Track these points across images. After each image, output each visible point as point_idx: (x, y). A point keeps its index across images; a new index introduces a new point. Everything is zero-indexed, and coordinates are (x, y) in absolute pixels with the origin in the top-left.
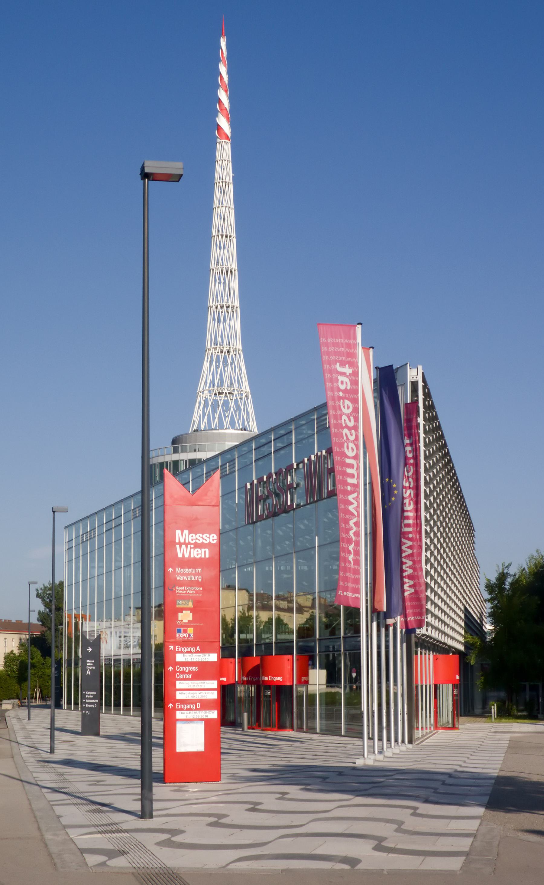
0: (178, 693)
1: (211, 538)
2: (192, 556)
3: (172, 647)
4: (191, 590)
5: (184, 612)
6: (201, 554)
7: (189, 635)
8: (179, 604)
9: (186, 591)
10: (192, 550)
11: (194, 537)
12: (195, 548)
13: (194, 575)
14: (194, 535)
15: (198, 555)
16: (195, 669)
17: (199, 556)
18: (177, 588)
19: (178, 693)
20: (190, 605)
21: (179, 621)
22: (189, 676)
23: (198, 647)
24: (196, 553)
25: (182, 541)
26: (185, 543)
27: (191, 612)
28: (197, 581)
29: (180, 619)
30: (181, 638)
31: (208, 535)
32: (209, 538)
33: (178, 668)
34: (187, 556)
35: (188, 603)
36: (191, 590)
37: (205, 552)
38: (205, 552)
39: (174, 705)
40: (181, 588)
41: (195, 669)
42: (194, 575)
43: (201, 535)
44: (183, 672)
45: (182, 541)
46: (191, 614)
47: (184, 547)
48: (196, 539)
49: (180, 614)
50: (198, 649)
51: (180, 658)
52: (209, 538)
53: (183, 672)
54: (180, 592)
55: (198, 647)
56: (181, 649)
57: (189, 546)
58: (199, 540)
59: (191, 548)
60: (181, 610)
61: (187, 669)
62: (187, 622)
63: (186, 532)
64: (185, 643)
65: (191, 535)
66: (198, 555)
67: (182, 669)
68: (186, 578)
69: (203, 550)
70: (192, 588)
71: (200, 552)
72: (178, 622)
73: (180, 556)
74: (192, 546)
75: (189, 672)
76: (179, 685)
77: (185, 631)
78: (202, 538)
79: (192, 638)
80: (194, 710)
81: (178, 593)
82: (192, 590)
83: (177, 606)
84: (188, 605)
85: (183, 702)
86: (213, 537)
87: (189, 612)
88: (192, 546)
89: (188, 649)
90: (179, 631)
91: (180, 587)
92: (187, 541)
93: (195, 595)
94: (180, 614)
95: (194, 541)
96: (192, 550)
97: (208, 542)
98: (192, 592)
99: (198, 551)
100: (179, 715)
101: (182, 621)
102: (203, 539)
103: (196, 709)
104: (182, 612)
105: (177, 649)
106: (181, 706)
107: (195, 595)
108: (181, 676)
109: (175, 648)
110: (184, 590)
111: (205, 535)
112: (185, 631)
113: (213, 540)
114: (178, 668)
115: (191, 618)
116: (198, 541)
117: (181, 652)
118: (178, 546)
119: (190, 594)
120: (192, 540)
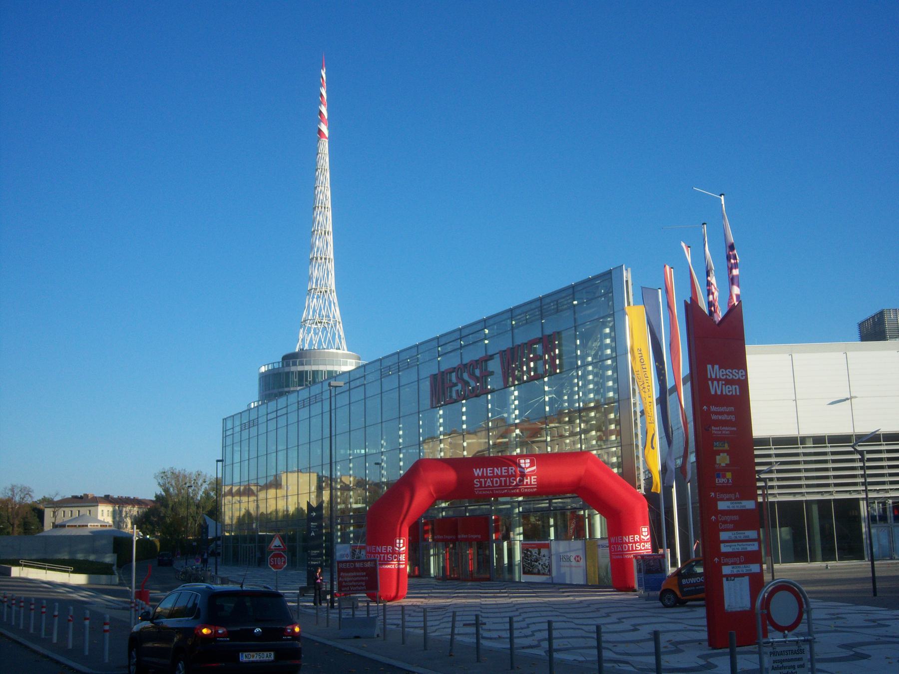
0: (722, 545)
1: (740, 374)
2: (724, 393)
3: (713, 494)
4: (726, 430)
5: (721, 454)
6: (732, 391)
7: (728, 480)
8: (716, 446)
9: (721, 431)
10: (724, 386)
11: (725, 373)
12: (725, 385)
13: (729, 413)
14: (724, 370)
15: (729, 391)
16: (736, 518)
17: (731, 393)
18: (713, 427)
19: (722, 545)
20: (726, 447)
21: (718, 464)
22: (731, 526)
23: (737, 493)
24: (727, 390)
25: (713, 377)
26: (716, 379)
27: (727, 455)
28: (731, 420)
29: (718, 462)
30: (720, 483)
31: (737, 371)
32: (738, 373)
33: (720, 518)
34: (719, 392)
35: (725, 443)
36: (726, 430)
37: (736, 388)
38: (736, 388)
39: (719, 558)
40: (716, 428)
41: (736, 518)
42: (729, 413)
43: (731, 371)
44: (725, 522)
45: (713, 377)
46: (728, 457)
47: (715, 383)
48: (727, 374)
49: (718, 457)
50: (738, 495)
51: (722, 505)
52: (738, 373)
53: (725, 522)
54: (716, 432)
55: (737, 493)
56: (722, 496)
57: (720, 382)
58: (729, 376)
59: (722, 384)
60: (718, 453)
61: (728, 518)
62: (724, 465)
63: (716, 367)
64: (724, 489)
65: (721, 370)
66: (729, 391)
67: (724, 518)
68: (720, 417)
69: (734, 387)
70: (727, 428)
71: (730, 389)
72: (716, 466)
73: (713, 392)
74: (724, 382)
75: (732, 522)
76: (724, 536)
77: (724, 476)
78: (732, 373)
79: (730, 483)
80: (739, 564)
81: (714, 434)
82: (728, 431)
83: (715, 448)
84: (724, 447)
85: (728, 555)
86: (742, 372)
87: (725, 454)
88: (724, 382)
89: (728, 496)
90: (718, 477)
91: (716, 427)
92: (718, 377)
93: (730, 435)
94: (718, 457)
95: (725, 377)
96: (724, 386)
97: (737, 378)
98: (727, 432)
99: (729, 388)
100: (726, 570)
101: (720, 464)
102: (733, 375)
103: (741, 563)
104: (720, 455)
105: (718, 495)
106: (726, 560)
107: (730, 435)
108: (724, 526)
109: (715, 495)
110: (720, 430)
111: (734, 370)
112: (724, 476)
113: (742, 376)
114: (720, 518)
115: (728, 462)
116: (728, 377)
117: (722, 500)
118: (710, 382)
119: (725, 434)
120: (723, 375)
